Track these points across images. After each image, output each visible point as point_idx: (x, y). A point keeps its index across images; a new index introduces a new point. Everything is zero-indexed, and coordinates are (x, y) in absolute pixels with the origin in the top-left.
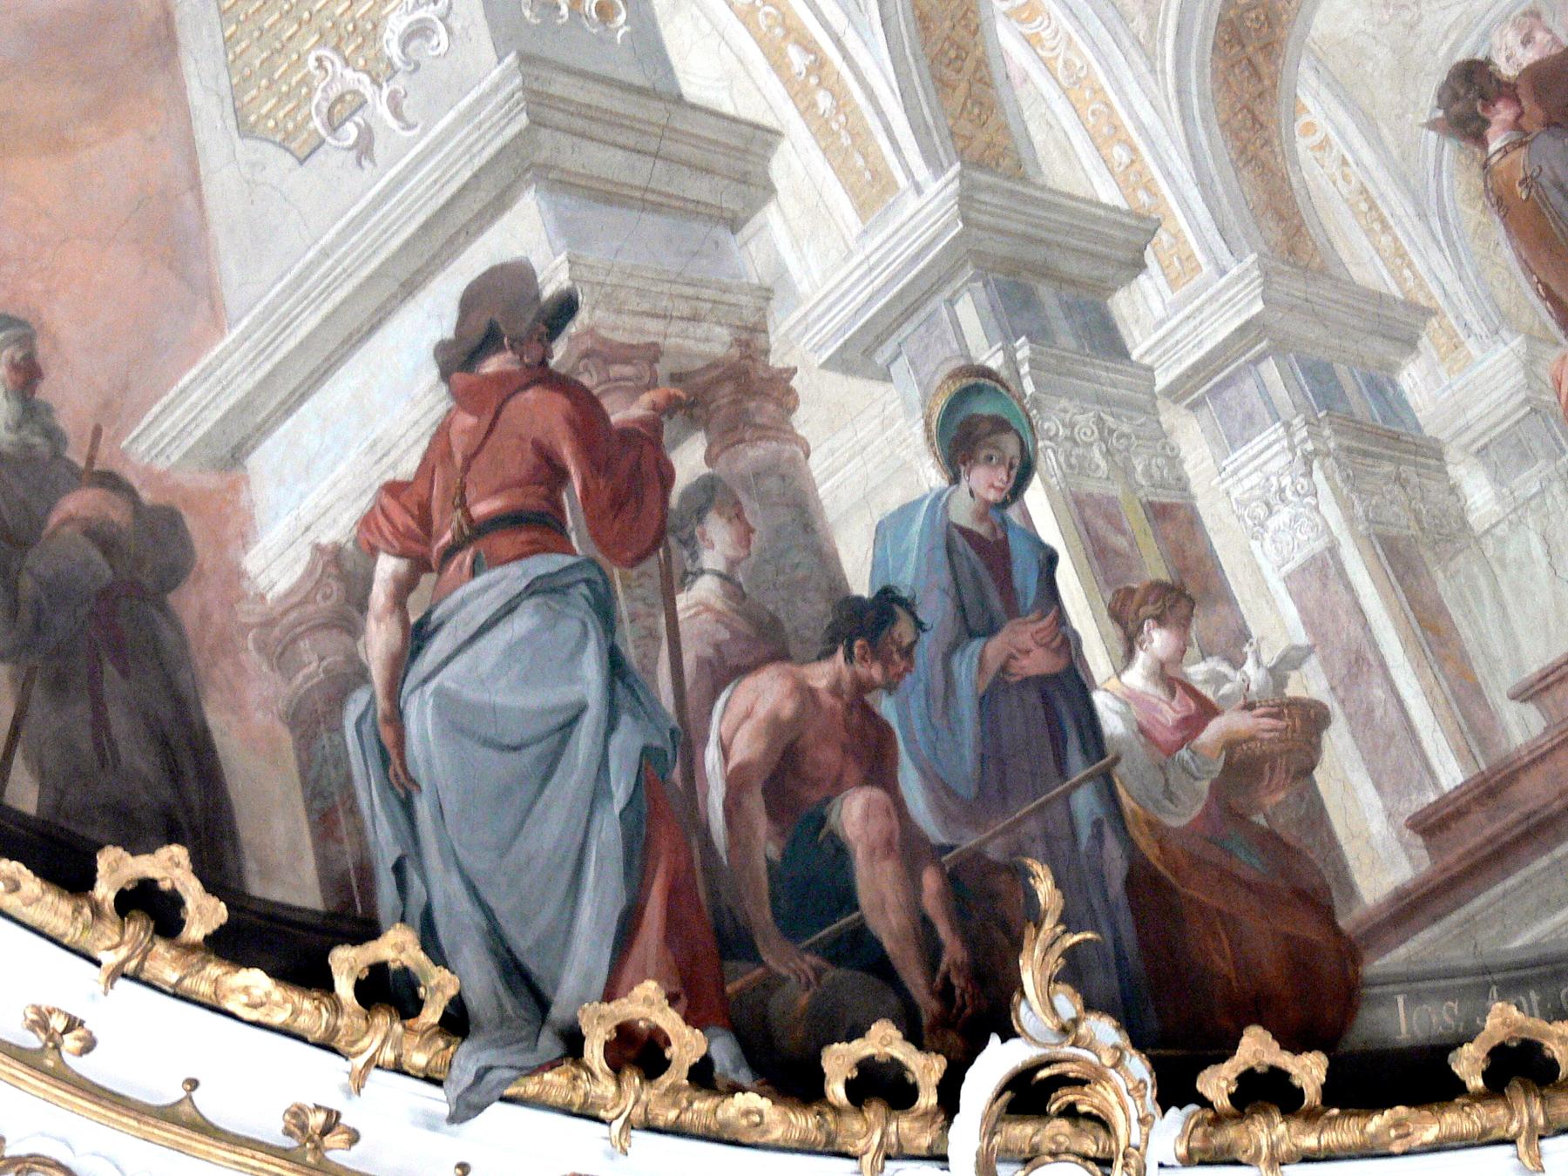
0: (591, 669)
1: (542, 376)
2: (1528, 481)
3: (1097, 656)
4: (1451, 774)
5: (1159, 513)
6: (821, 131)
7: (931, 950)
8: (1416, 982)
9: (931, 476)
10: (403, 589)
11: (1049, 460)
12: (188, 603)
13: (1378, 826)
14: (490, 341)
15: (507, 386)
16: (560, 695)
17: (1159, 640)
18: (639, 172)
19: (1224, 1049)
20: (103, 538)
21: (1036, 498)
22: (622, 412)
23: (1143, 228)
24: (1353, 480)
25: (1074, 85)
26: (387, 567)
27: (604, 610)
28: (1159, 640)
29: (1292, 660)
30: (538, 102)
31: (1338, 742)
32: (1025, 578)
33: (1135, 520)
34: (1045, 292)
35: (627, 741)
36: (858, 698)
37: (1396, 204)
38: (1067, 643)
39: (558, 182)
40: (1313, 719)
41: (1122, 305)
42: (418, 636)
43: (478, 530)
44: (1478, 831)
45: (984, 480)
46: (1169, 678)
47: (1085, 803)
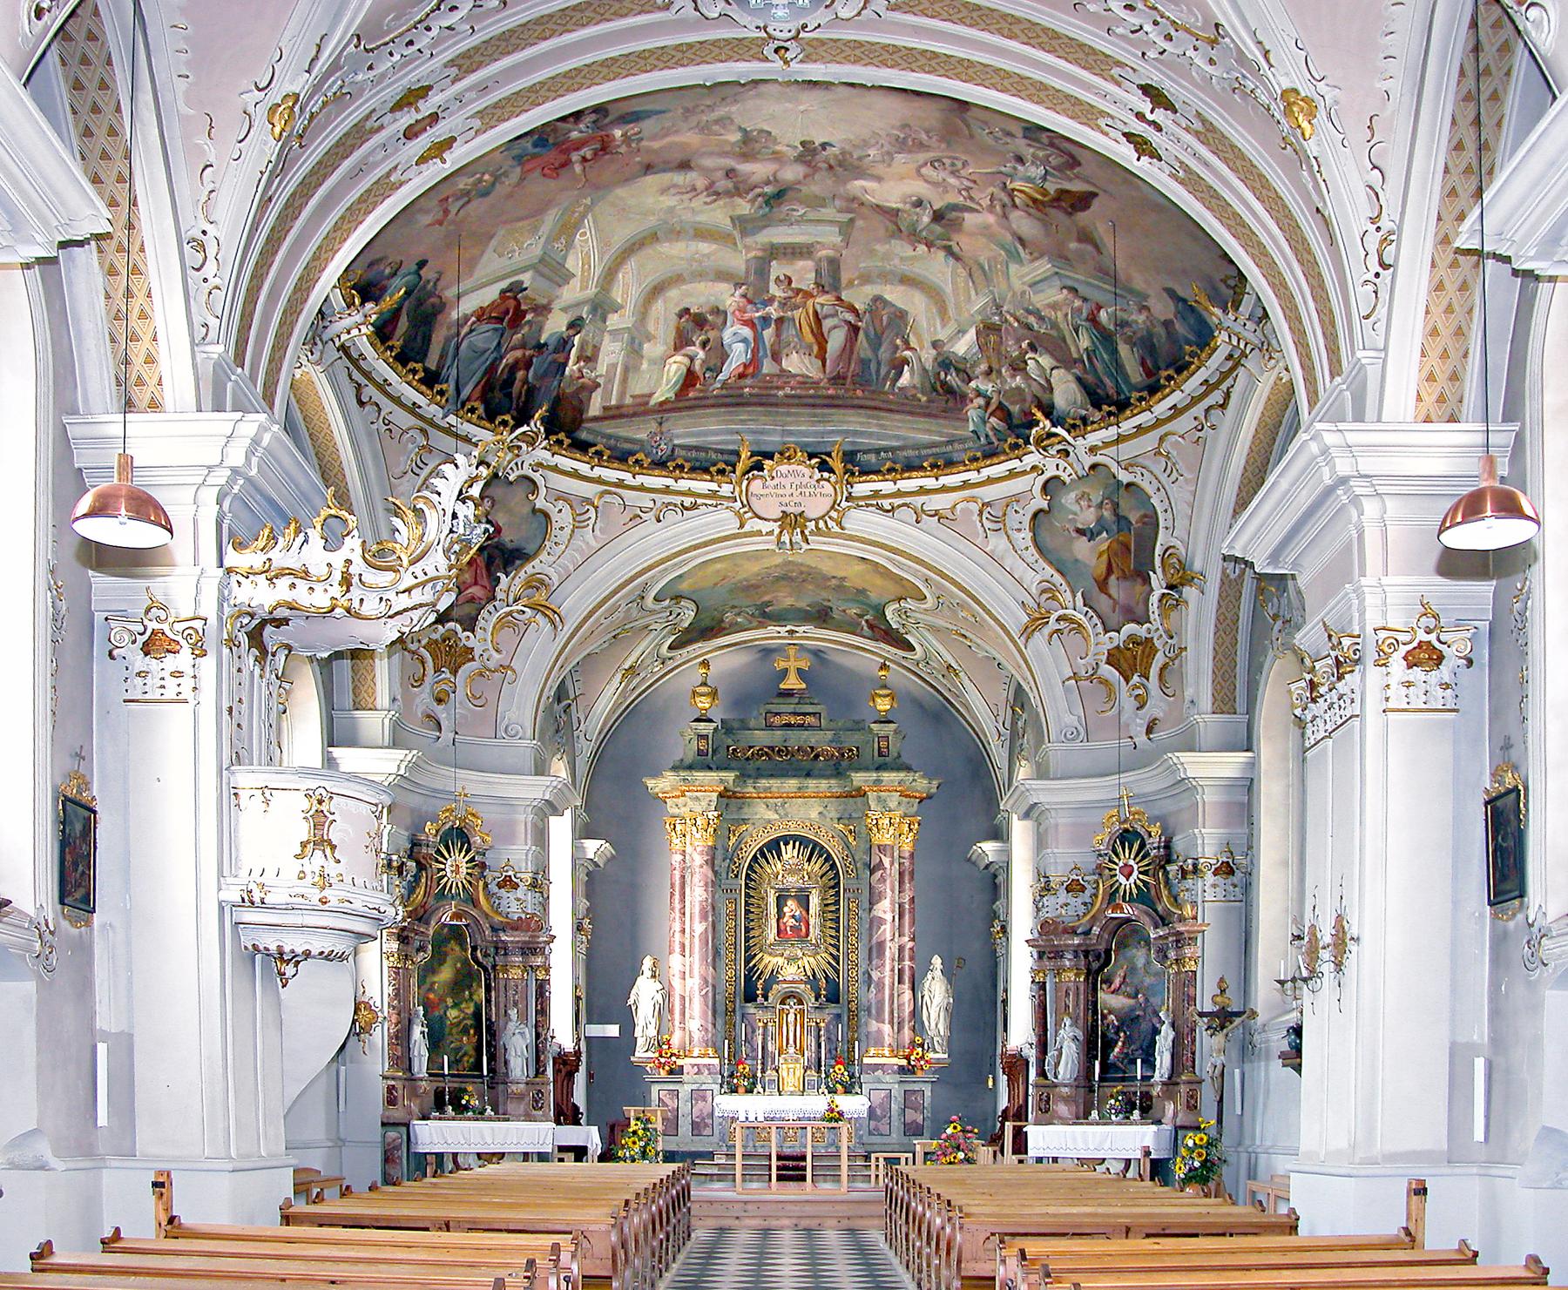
0: (495, 343)
1: (515, 298)
2: (653, 367)
3: (571, 362)
4: (613, 402)
5: (595, 346)
6: (582, 282)
7: (519, 397)
8: (589, 431)
9: (564, 329)
10: (474, 323)
11: (583, 332)
12: (440, 317)
13: (598, 405)
14: (510, 291)
15: (509, 298)
16: (486, 346)
17: (582, 363)
18: (552, 275)
19: (557, 434)
20: (433, 306)
21: (577, 338)
22: (523, 307)
23: (622, 307)
24: (628, 356)
25: (626, 285)
26: (474, 319)
27: (502, 335)
28: (582, 363)
29: (601, 376)
30: (542, 260)
31: (599, 390)
32: (568, 348)
33: (590, 347)
34: (599, 311)
35: (495, 355)
36: (531, 358)
37: (662, 322)
38: (568, 358)
39: (537, 271)
40: (598, 385)
41: (610, 316)
42: (471, 331)
43: (490, 318)
44: (611, 413)
45: (571, 332)
46: (580, 370)
47: (556, 383)
